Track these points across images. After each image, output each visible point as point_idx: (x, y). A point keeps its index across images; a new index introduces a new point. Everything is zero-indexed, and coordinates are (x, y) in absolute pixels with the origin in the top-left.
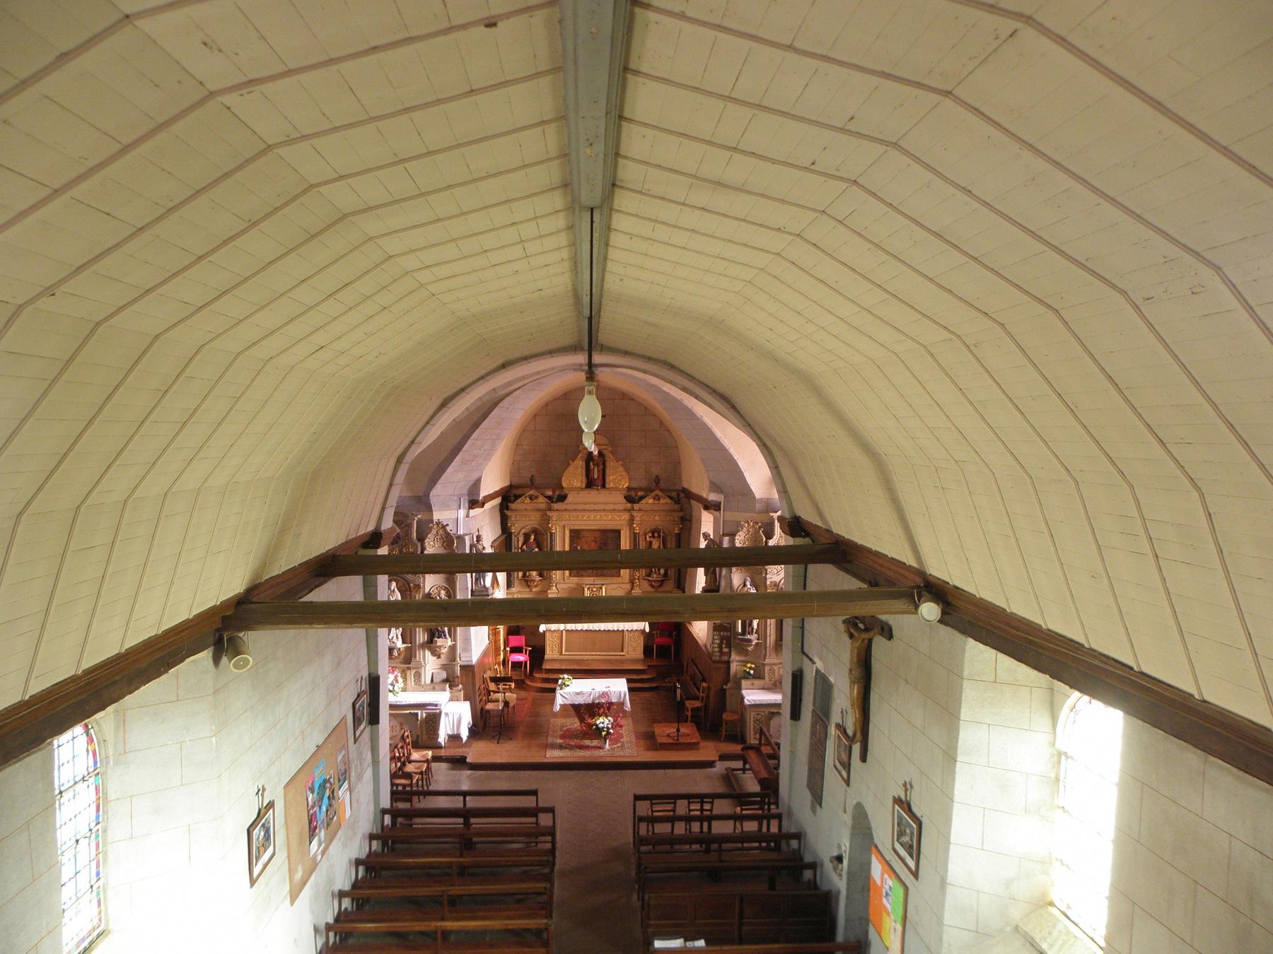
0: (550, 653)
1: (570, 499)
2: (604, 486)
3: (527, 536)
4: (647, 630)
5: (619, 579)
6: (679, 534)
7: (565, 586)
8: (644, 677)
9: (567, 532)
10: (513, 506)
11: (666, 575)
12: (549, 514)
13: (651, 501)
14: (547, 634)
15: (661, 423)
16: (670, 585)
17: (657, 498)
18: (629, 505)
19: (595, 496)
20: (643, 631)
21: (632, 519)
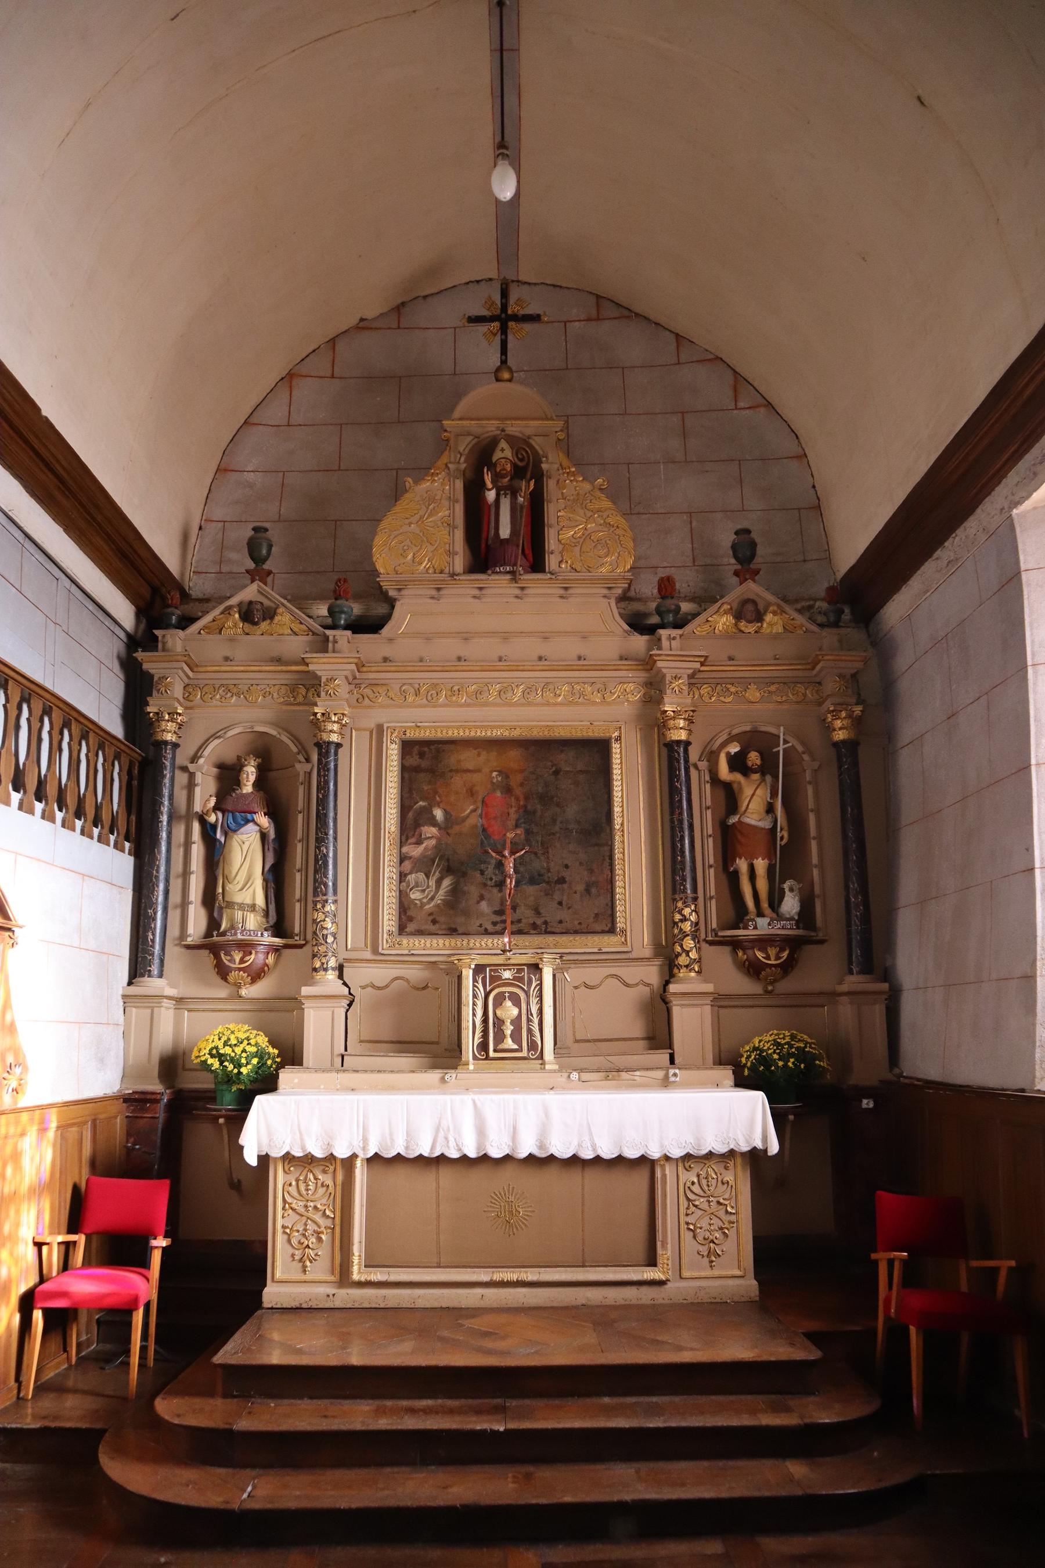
0: (291, 1276)
1: (402, 620)
2: (537, 565)
3: (228, 775)
5: (610, 943)
6: (847, 754)
7: (381, 974)
9: (393, 753)
10: (175, 639)
11: (806, 916)
12: (321, 665)
13: (724, 622)
14: (279, 1178)
15: (739, 381)
16: (823, 970)
17: (749, 612)
18: (639, 642)
19: (502, 606)
21: (654, 689)
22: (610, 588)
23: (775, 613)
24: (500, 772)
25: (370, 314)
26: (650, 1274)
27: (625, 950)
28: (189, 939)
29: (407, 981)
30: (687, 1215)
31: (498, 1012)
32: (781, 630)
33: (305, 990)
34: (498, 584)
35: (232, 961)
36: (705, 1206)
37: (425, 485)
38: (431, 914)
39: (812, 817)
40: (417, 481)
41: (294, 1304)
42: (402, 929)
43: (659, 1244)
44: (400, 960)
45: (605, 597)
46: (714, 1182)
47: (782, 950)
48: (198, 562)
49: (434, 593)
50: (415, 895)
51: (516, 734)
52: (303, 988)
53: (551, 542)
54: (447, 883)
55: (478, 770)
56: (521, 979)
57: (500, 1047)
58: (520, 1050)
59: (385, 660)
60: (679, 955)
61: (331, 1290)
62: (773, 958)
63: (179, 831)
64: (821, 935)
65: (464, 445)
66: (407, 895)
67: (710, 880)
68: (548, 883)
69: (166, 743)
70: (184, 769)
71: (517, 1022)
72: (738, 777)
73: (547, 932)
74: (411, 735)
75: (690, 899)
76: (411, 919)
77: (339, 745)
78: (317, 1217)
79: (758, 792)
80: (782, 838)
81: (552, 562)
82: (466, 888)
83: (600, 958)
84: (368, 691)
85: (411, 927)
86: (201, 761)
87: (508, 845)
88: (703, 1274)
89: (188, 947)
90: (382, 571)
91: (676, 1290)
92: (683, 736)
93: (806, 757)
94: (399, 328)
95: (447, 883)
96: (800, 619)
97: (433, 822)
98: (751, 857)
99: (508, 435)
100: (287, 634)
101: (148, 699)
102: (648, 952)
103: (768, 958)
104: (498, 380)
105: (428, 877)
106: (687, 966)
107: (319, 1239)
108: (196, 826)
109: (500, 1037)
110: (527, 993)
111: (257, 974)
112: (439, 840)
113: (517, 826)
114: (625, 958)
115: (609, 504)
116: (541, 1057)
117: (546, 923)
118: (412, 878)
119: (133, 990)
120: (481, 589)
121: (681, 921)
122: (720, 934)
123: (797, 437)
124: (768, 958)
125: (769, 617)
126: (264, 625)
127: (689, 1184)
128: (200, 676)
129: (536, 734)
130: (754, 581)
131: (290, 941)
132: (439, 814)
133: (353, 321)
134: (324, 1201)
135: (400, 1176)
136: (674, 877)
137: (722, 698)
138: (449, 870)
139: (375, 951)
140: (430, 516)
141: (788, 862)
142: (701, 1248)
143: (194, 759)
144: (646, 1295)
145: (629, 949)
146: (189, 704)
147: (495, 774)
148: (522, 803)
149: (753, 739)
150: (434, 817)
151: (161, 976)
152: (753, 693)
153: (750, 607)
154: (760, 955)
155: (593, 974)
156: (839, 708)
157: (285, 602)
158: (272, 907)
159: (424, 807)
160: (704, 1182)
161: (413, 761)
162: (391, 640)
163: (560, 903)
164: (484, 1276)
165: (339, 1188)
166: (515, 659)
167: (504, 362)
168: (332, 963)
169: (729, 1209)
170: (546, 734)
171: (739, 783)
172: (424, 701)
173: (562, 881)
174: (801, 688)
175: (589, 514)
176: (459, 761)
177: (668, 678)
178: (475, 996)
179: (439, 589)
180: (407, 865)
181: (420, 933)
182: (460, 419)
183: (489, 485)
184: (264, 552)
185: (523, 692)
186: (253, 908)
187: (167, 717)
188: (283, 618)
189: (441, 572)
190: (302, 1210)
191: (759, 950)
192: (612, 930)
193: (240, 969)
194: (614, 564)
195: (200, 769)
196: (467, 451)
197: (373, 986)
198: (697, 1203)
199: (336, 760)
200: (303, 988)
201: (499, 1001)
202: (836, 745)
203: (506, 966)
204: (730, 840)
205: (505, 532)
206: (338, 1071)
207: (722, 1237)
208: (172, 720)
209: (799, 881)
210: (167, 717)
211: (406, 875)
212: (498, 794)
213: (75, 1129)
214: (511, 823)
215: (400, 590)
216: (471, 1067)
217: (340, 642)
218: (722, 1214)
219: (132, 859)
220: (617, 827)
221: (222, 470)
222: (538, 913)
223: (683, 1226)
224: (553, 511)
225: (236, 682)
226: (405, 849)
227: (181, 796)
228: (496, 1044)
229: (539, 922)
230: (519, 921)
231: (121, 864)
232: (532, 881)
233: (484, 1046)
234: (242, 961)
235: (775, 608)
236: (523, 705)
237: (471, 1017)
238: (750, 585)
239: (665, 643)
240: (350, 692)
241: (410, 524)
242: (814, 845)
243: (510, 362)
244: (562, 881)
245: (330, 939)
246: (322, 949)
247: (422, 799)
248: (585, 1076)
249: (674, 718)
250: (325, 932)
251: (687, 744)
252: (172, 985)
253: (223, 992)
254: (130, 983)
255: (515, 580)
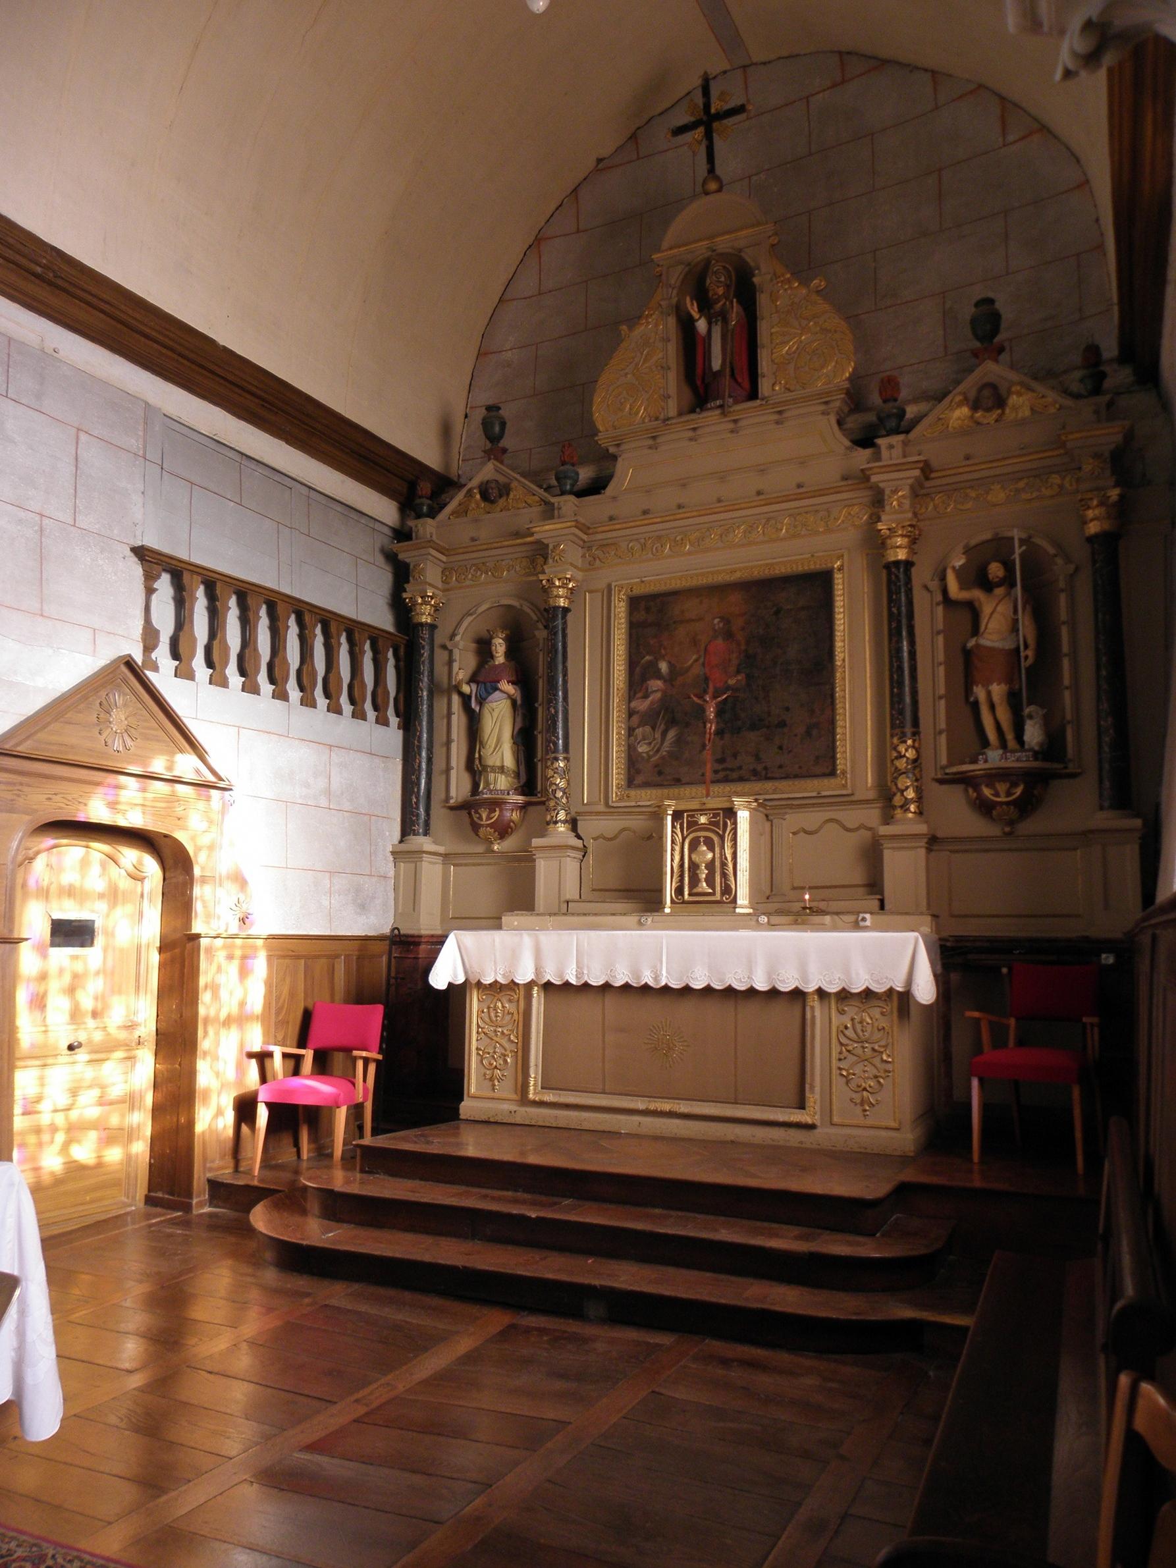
0: (482, 1091)
1: (625, 475)
3: (483, 647)
4: (925, 990)
5: (828, 787)
7: (609, 825)
8: (839, 1246)
9: (620, 609)
11: (1053, 748)
14: (474, 1003)
15: (1007, 106)
16: (1078, 805)
17: (992, 398)
20: (903, 1000)
22: (826, 403)
23: (1019, 394)
24: (722, 618)
25: (605, 152)
26: (797, 1116)
27: (844, 792)
28: (452, 801)
29: (634, 832)
30: (840, 1060)
31: (694, 856)
32: (1027, 413)
33: (536, 842)
34: (710, 419)
35: (480, 818)
36: (859, 1051)
37: (639, 330)
38: (656, 766)
39: (1064, 632)
40: (631, 329)
41: (483, 1118)
42: (630, 782)
43: (807, 1086)
44: (627, 812)
45: (823, 413)
46: (869, 1028)
47: (1014, 785)
48: (465, 449)
49: (651, 442)
50: (642, 749)
51: (736, 577)
52: (534, 840)
53: (764, 365)
54: (672, 734)
55: (701, 619)
56: (716, 824)
57: (695, 891)
58: (713, 894)
59: (611, 518)
60: (895, 794)
61: (513, 1107)
62: (1002, 794)
63: (440, 705)
64: (1071, 768)
65: (675, 277)
66: (635, 749)
67: (934, 711)
68: (768, 727)
69: (422, 624)
70: (444, 647)
71: (710, 866)
72: (977, 594)
73: (767, 778)
74: (637, 591)
75: (909, 734)
76: (638, 772)
77: (566, 610)
78: (504, 1042)
79: (999, 609)
80: (1026, 657)
81: (764, 387)
82: (689, 739)
83: (820, 802)
84: (599, 553)
85: (639, 779)
86: (458, 638)
87: (711, 690)
88: (855, 1122)
89: (452, 808)
90: (601, 429)
91: (824, 1136)
92: (902, 555)
93: (1059, 561)
94: (638, 159)
95: (672, 734)
96: (1051, 396)
97: (658, 675)
98: (986, 684)
99: (722, 254)
100: (521, 509)
101: (406, 586)
102: (871, 795)
103: (997, 794)
104: (707, 193)
105: (653, 728)
106: (901, 807)
107: (505, 1061)
108: (456, 699)
109: (694, 881)
110: (722, 838)
111: (503, 831)
112: (664, 692)
113: (738, 672)
114: (847, 801)
115: (827, 307)
116: (734, 900)
117: (766, 768)
118: (639, 731)
119: (404, 847)
120: (694, 429)
121: (897, 758)
122: (947, 771)
123: (1078, 161)
124: (997, 794)
125: (1013, 400)
126: (502, 502)
127: (842, 1028)
128: (452, 559)
129: (757, 574)
130: (996, 361)
131: (534, 799)
132: (663, 667)
133: (591, 163)
134: (510, 1027)
135: (585, 1010)
136: (899, 712)
137: (959, 506)
138: (672, 722)
139: (607, 804)
140: (645, 361)
141: (1034, 681)
142: (854, 1095)
143: (453, 635)
144: (794, 1138)
145: (849, 792)
146: (447, 586)
147: (716, 621)
148: (743, 647)
149: (999, 547)
150: (659, 670)
151: (426, 834)
152: (998, 495)
153: (986, 393)
154: (987, 792)
155: (812, 818)
156: (1089, 495)
157: (518, 477)
158: (522, 768)
159: (650, 662)
160: (859, 1027)
161: (641, 616)
162: (614, 498)
163: (780, 748)
164: (640, 1105)
165: (521, 1019)
166: (735, 496)
167: (711, 170)
168: (562, 815)
169: (885, 1057)
170: (767, 573)
171: (979, 600)
172: (650, 555)
173: (782, 724)
174: (1056, 479)
175: (804, 323)
176: (683, 612)
177: (887, 492)
178: (673, 842)
179: (654, 438)
180: (635, 719)
181: (647, 785)
182: (671, 249)
183: (696, 315)
184: (497, 429)
185: (745, 532)
186: (502, 769)
187: (420, 601)
188: (517, 493)
189: (657, 419)
190: (492, 1034)
191: (987, 786)
192: (832, 773)
193: (488, 825)
194: (837, 372)
195: (456, 646)
196: (678, 284)
197: (604, 838)
198: (850, 1048)
199: (565, 623)
200: (534, 840)
201: (694, 847)
202: (1090, 540)
203: (702, 811)
204: (967, 665)
205: (716, 364)
206: (564, 914)
207: (877, 1087)
208: (425, 603)
209: (1042, 706)
210: (420, 601)
211: (634, 729)
212: (720, 641)
213: (323, 961)
214: (732, 669)
215: (618, 445)
216: (667, 910)
217: (564, 508)
218: (877, 1061)
219: (401, 732)
220: (838, 663)
221: (481, 354)
222: (757, 758)
223: (835, 1071)
224: (764, 329)
225: (483, 560)
226: (633, 704)
227: (440, 670)
228: (692, 886)
229: (759, 768)
230: (740, 768)
231: (392, 736)
232: (753, 727)
233: (679, 891)
234: (489, 818)
235: (1018, 388)
236: (743, 545)
237: (670, 862)
238: (990, 365)
239: (885, 453)
240: (583, 556)
241: (626, 374)
242: (1066, 663)
243: (718, 171)
244: (782, 724)
245: (559, 794)
246: (552, 803)
247: (648, 653)
248: (775, 919)
249: (889, 537)
250: (554, 787)
251: (908, 564)
252: (435, 843)
253: (480, 849)
254: (401, 841)
255: (724, 414)
